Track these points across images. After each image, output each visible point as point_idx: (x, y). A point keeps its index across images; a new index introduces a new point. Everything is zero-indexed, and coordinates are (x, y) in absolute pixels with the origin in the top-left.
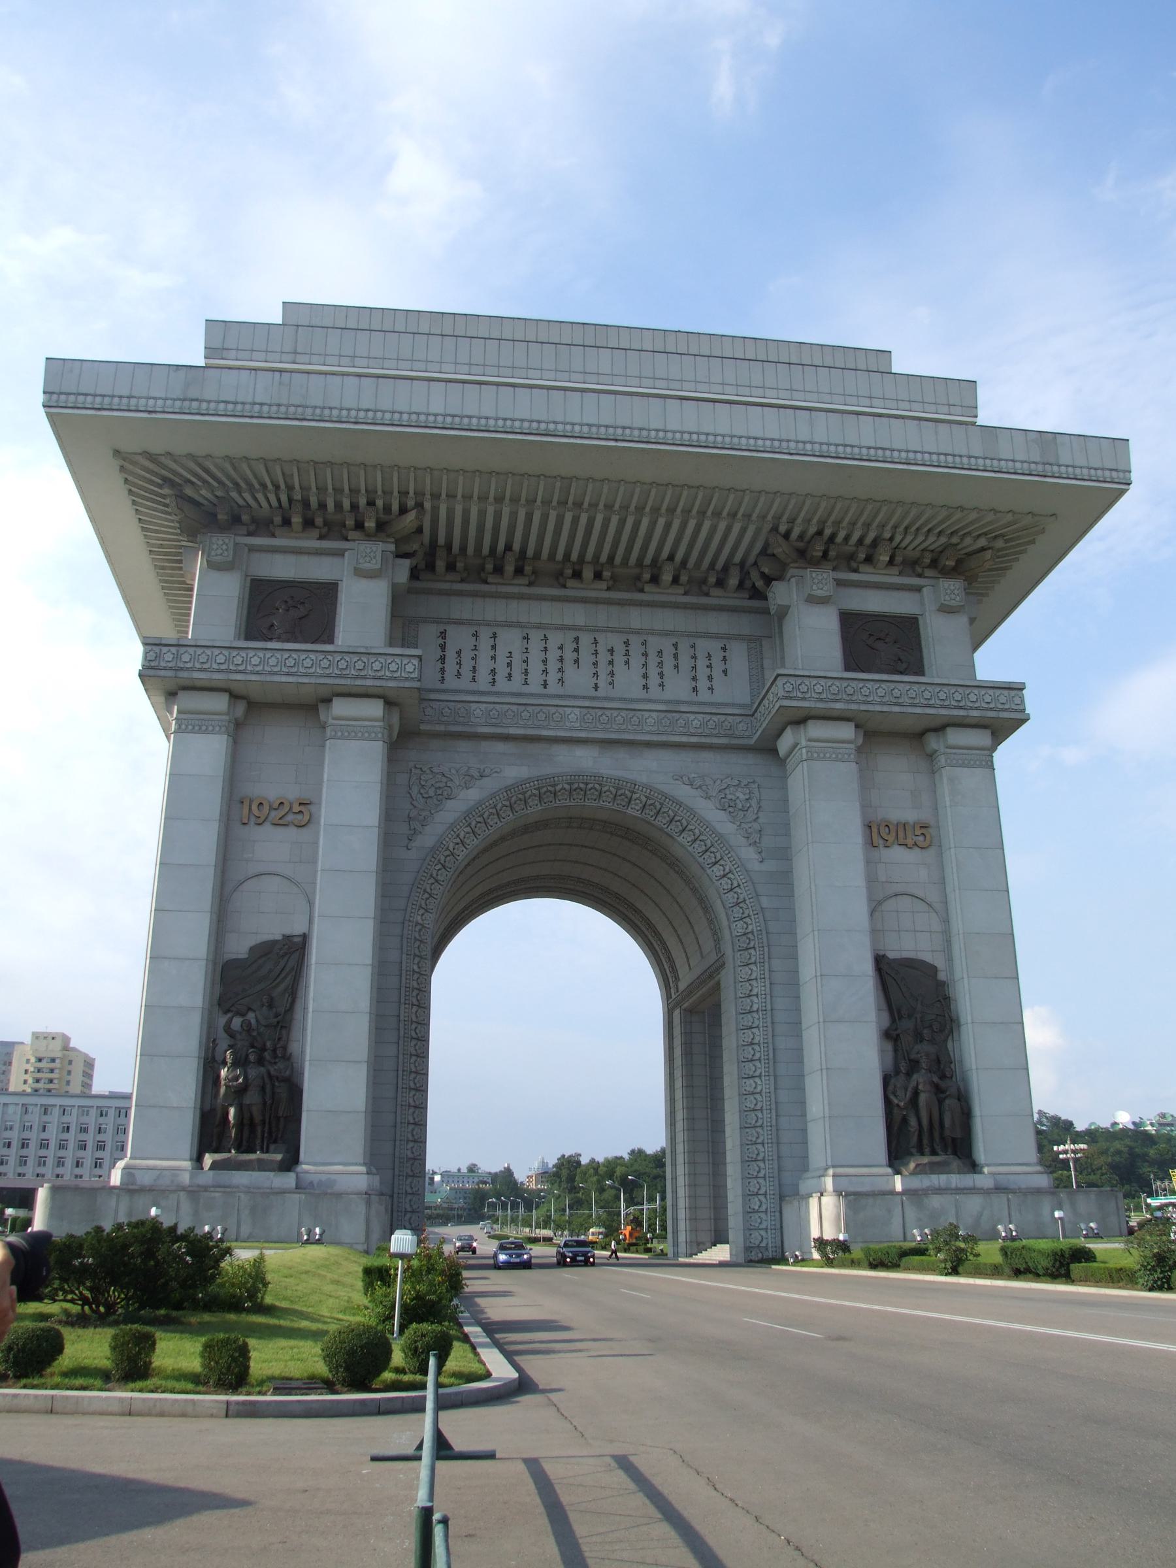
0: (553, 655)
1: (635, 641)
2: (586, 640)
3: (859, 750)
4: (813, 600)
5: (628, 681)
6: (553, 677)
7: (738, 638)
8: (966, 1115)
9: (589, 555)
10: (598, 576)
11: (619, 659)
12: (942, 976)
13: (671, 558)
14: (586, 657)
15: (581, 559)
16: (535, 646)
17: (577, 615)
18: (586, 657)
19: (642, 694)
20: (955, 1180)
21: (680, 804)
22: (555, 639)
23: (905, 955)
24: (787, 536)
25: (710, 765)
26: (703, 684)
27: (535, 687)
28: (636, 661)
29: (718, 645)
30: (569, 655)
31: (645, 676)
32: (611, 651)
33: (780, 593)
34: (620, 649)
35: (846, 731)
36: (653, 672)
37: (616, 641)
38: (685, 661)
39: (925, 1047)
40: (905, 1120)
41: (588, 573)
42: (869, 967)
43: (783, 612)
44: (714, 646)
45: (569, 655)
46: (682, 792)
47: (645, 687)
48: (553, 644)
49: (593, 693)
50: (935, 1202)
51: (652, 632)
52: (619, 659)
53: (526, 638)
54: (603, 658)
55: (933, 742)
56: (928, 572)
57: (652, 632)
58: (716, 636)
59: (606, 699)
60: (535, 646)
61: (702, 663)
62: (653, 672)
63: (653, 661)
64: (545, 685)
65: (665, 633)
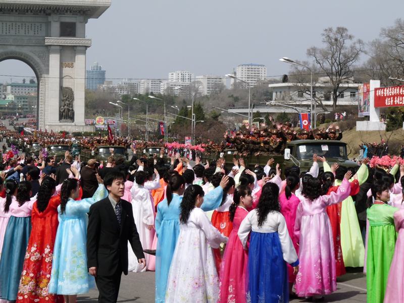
0: (8, 27)
1: (24, 24)
2: (14, 24)
3: (61, 50)
4: (54, 21)
5: (22, 32)
6: (8, 32)
7: (44, 23)
8: (73, 114)
9: (14, 8)
10: (16, 11)
11: (20, 28)
12: (73, 90)
13: (30, 8)
14: (14, 27)
15: (13, 9)
16: (4, 25)
17: (13, 19)
18: (14, 27)
19: (24, 35)
20: (68, 124)
21: (30, 56)
22: (8, 24)
23: (67, 86)
24: (50, 8)
25: (37, 49)
26: (36, 32)
27: (4, 34)
28: (24, 28)
29: (40, 24)
30: (11, 27)
31: (25, 31)
32: (19, 26)
33: (50, 18)
34: (21, 25)
35: (58, 48)
36: (27, 30)
37: (20, 24)
38: (33, 27)
39: (67, 102)
40: (63, 114)
41: (14, 11)
42: (58, 89)
43: (50, 22)
44: (39, 24)
45: (11, 27)
46: (31, 54)
47: (25, 33)
48: (8, 25)
49: (15, 34)
50: (63, 127)
51: (27, 22)
52: (20, 28)
53: (3, 24)
54: (17, 27)
55: (75, 47)
56: (79, 14)
57: (27, 22)
58: (40, 22)
59: (18, 36)
60: (4, 25)
61: (36, 28)
62: (27, 30)
63: (27, 28)
64: (6, 33)
65: (29, 22)
